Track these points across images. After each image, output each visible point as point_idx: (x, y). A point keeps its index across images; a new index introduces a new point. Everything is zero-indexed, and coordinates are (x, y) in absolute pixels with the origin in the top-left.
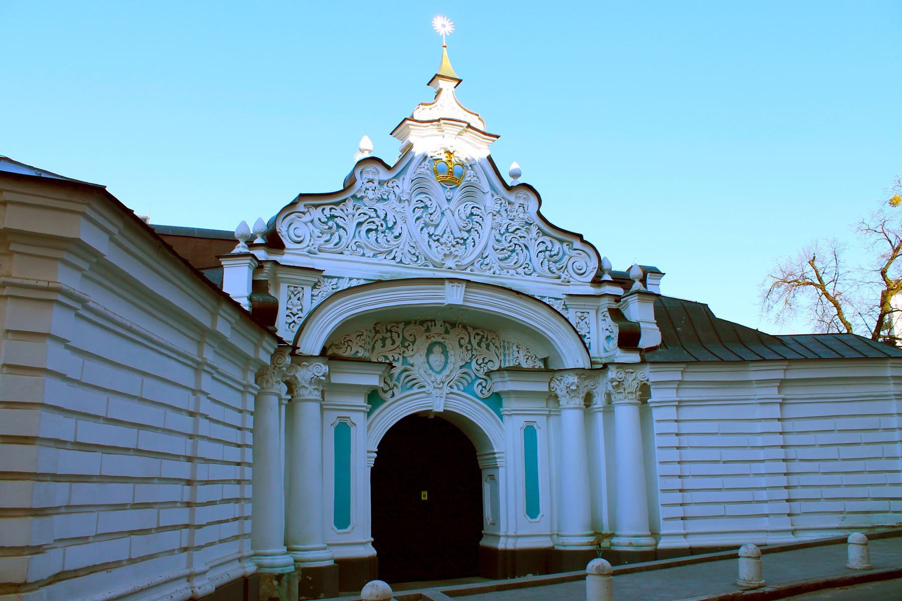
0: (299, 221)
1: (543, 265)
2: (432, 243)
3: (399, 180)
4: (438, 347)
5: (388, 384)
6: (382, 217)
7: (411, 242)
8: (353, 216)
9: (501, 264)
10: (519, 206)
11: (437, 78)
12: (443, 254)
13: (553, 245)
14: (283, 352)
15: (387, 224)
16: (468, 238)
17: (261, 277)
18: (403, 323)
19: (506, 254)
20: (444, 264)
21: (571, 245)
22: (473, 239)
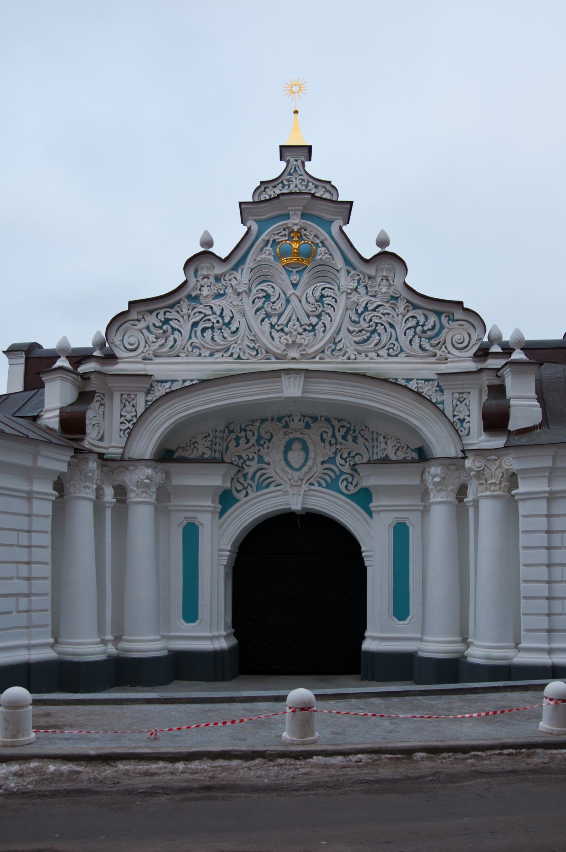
0: (133, 329)
1: (412, 343)
2: (275, 334)
3: (237, 271)
4: (296, 443)
5: (241, 484)
6: (218, 313)
7: (250, 335)
8: (189, 316)
9: (357, 347)
10: (382, 279)
11: (283, 149)
12: (285, 343)
13: (426, 318)
14: (86, 458)
15: (223, 320)
16: (317, 324)
17: (90, 388)
18: (259, 421)
19: (365, 335)
20: (287, 355)
21: (451, 316)
22: (323, 323)
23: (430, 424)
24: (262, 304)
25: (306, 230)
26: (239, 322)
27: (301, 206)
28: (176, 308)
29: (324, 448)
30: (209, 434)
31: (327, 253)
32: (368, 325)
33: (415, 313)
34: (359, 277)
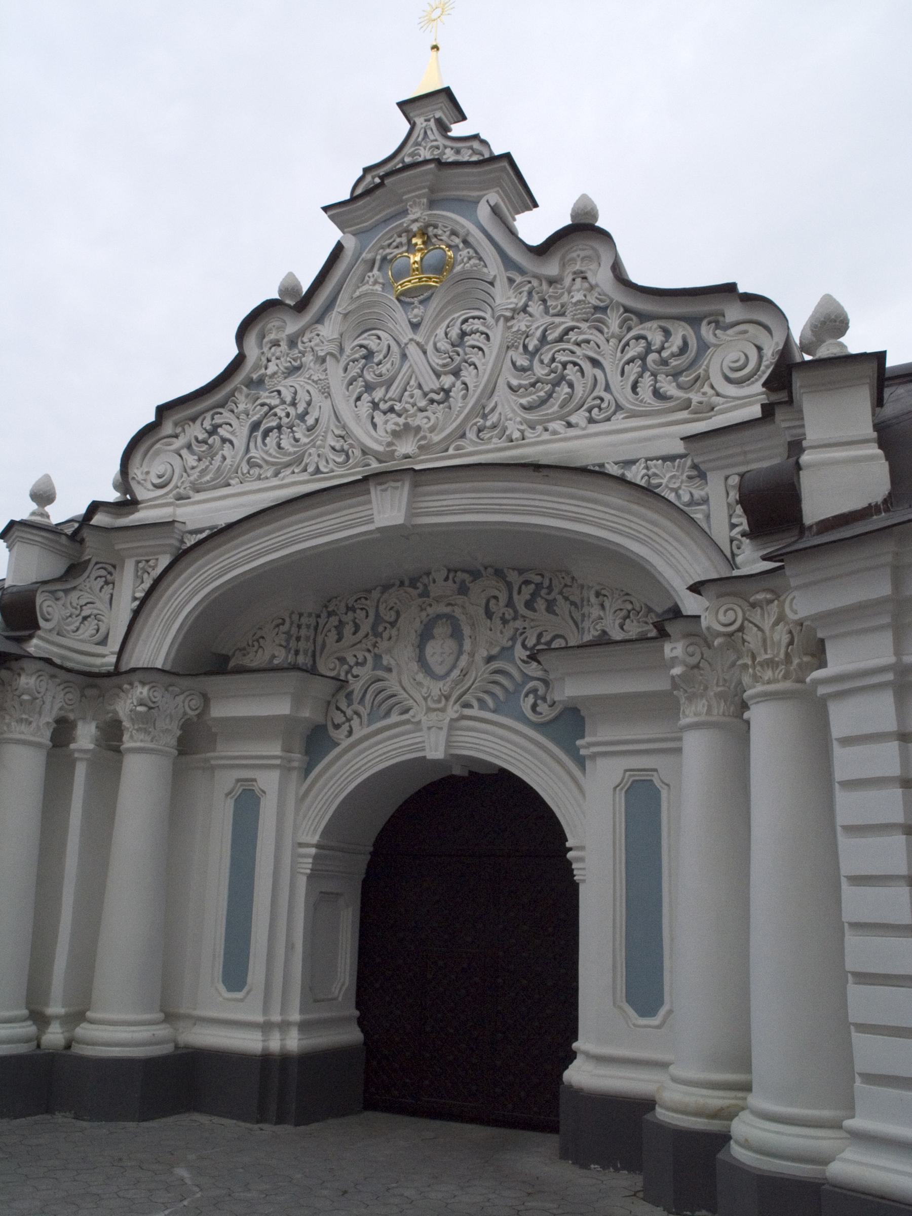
1: (638, 389)
2: (379, 418)
5: (343, 712)
6: (288, 399)
8: (248, 415)
10: (574, 280)
13: (667, 333)
16: (454, 385)
18: (379, 588)
23: (670, 548)
24: (359, 371)
25: (436, 227)
26: (320, 407)
27: (424, 188)
28: (231, 405)
29: (491, 630)
30: (284, 620)
31: (473, 258)
32: (546, 371)
33: (642, 329)
34: (530, 285)
